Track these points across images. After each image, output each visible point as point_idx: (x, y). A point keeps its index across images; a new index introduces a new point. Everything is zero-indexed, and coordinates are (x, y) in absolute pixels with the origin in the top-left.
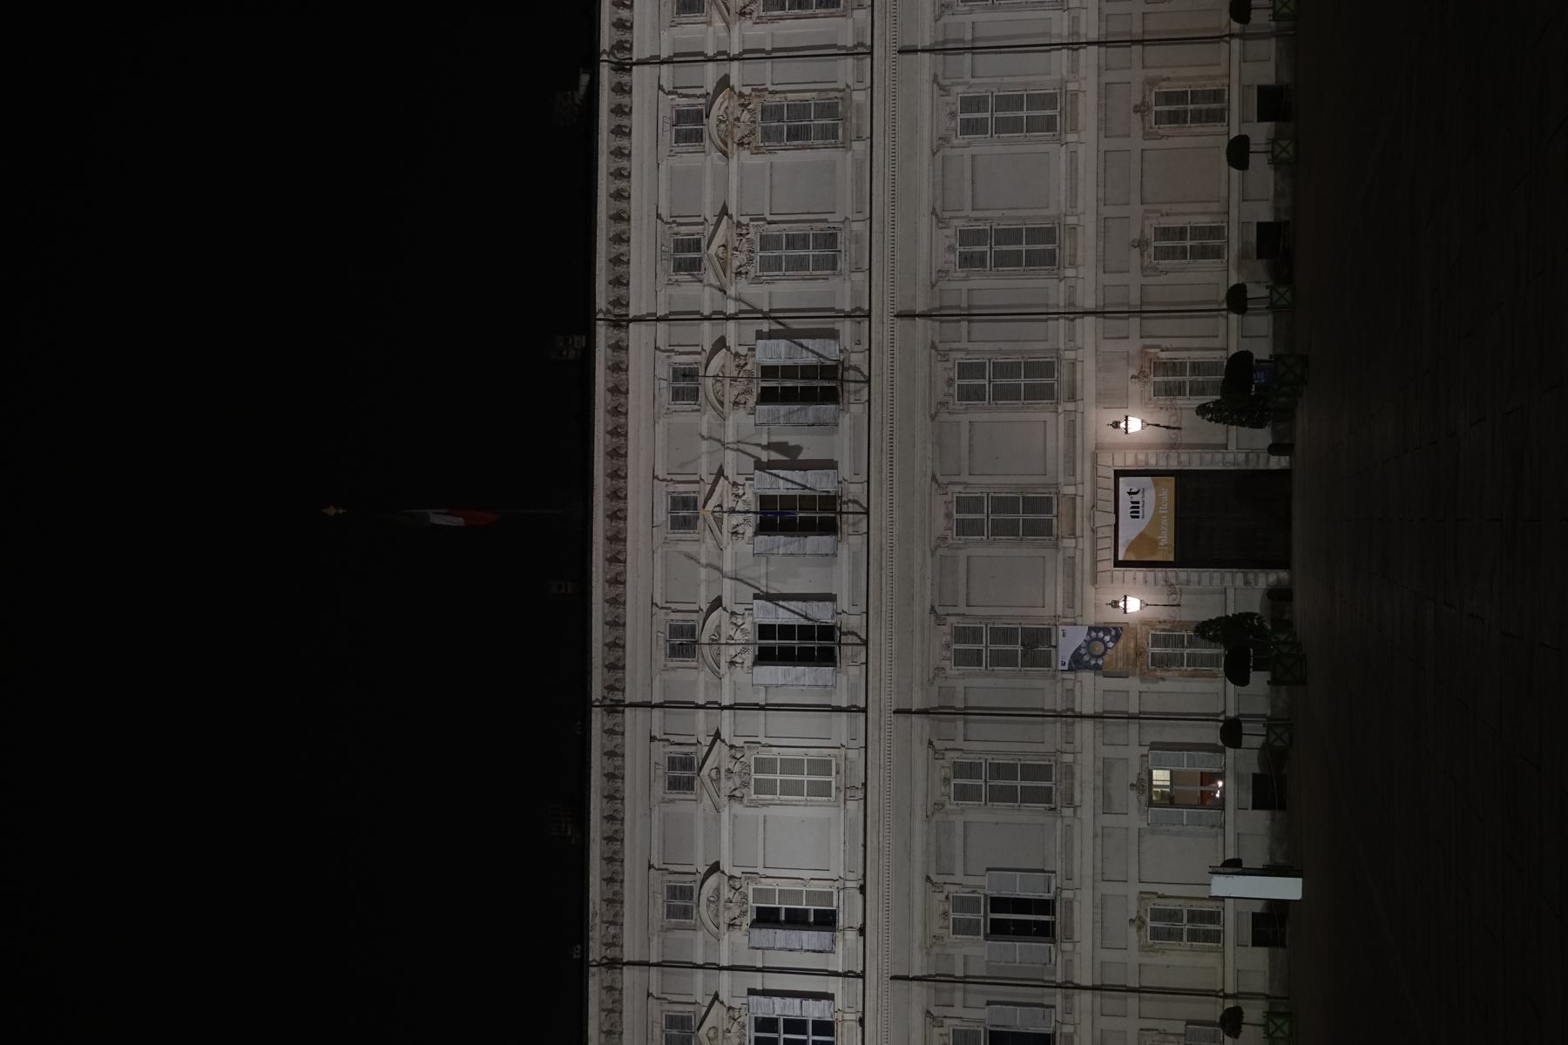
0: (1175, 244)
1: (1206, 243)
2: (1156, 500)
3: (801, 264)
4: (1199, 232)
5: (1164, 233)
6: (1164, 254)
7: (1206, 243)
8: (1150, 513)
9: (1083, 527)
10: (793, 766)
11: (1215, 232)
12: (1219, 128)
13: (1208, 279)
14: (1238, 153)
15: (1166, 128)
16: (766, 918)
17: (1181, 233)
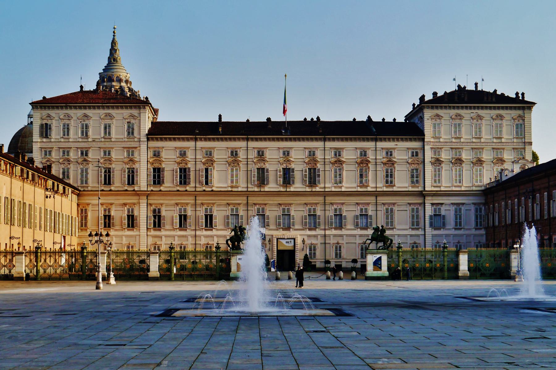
0: (338, 249)
1: (338, 255)
2: (289, 246)
3: (336, 177)
4: (340, 253)
5: (340, 247)
6: (336, 248)
7: (338, 255)
8: (287, 245)
9: (285, 232)
10: (237, 175)
11: (340, 257)
12: (360, 257)
13: (331, 255)
14: (355, 261)
15: (360, 247)
16: (207, 170)
17: (340, 250)
